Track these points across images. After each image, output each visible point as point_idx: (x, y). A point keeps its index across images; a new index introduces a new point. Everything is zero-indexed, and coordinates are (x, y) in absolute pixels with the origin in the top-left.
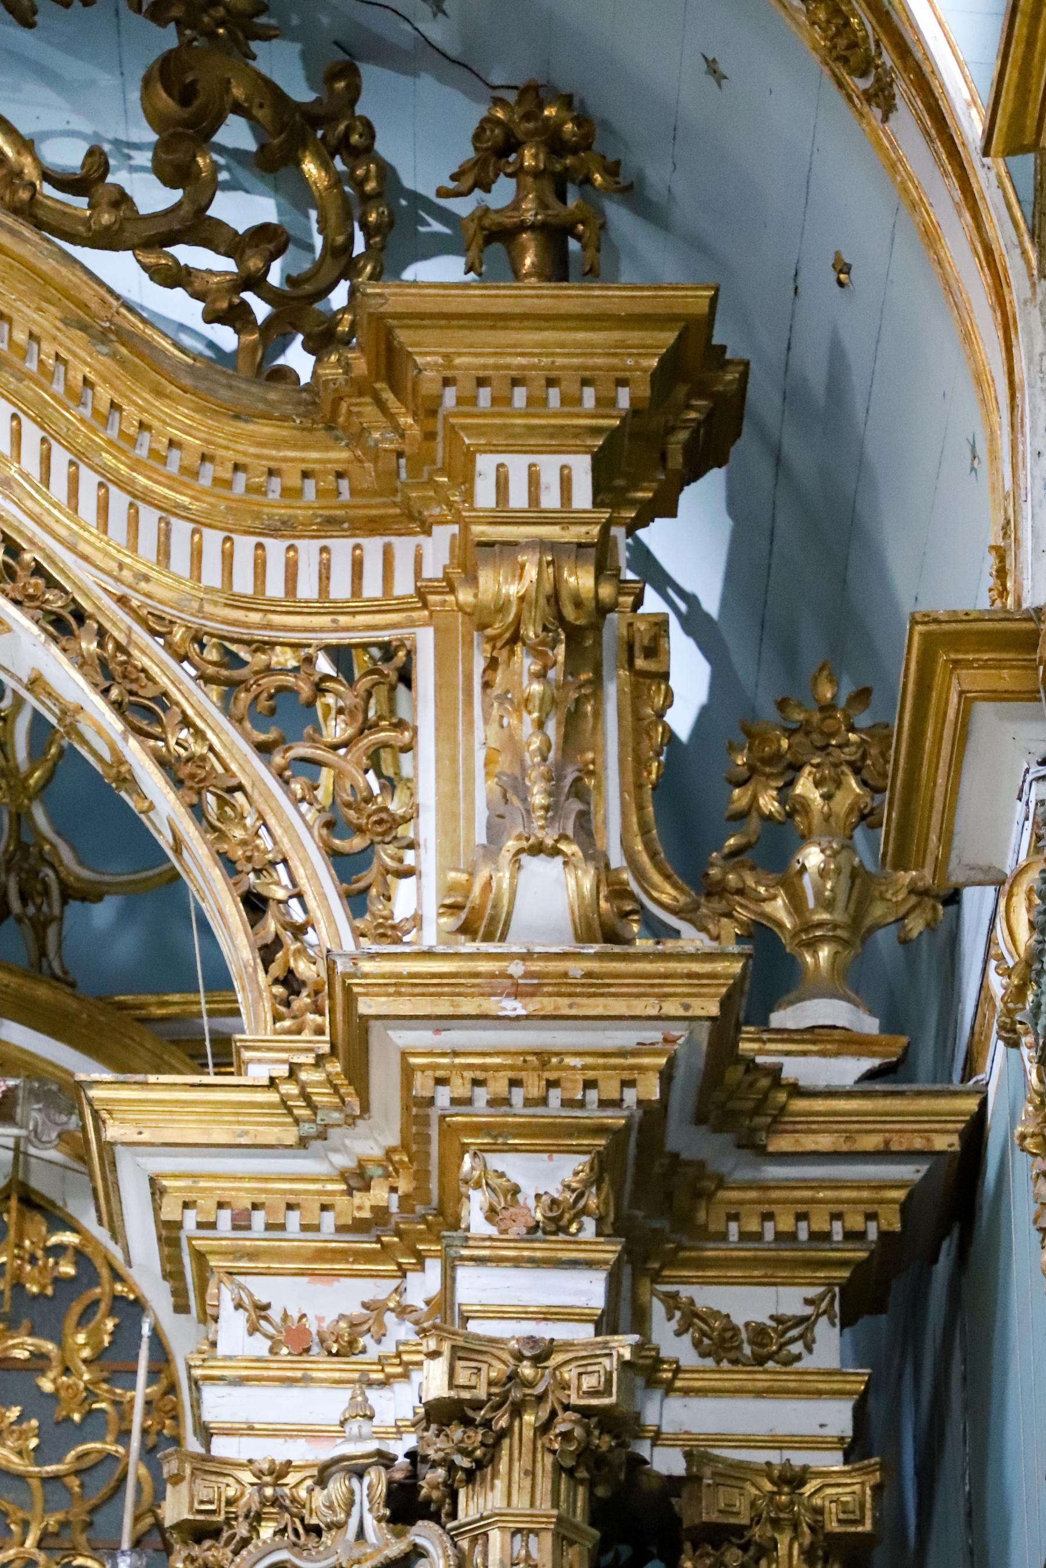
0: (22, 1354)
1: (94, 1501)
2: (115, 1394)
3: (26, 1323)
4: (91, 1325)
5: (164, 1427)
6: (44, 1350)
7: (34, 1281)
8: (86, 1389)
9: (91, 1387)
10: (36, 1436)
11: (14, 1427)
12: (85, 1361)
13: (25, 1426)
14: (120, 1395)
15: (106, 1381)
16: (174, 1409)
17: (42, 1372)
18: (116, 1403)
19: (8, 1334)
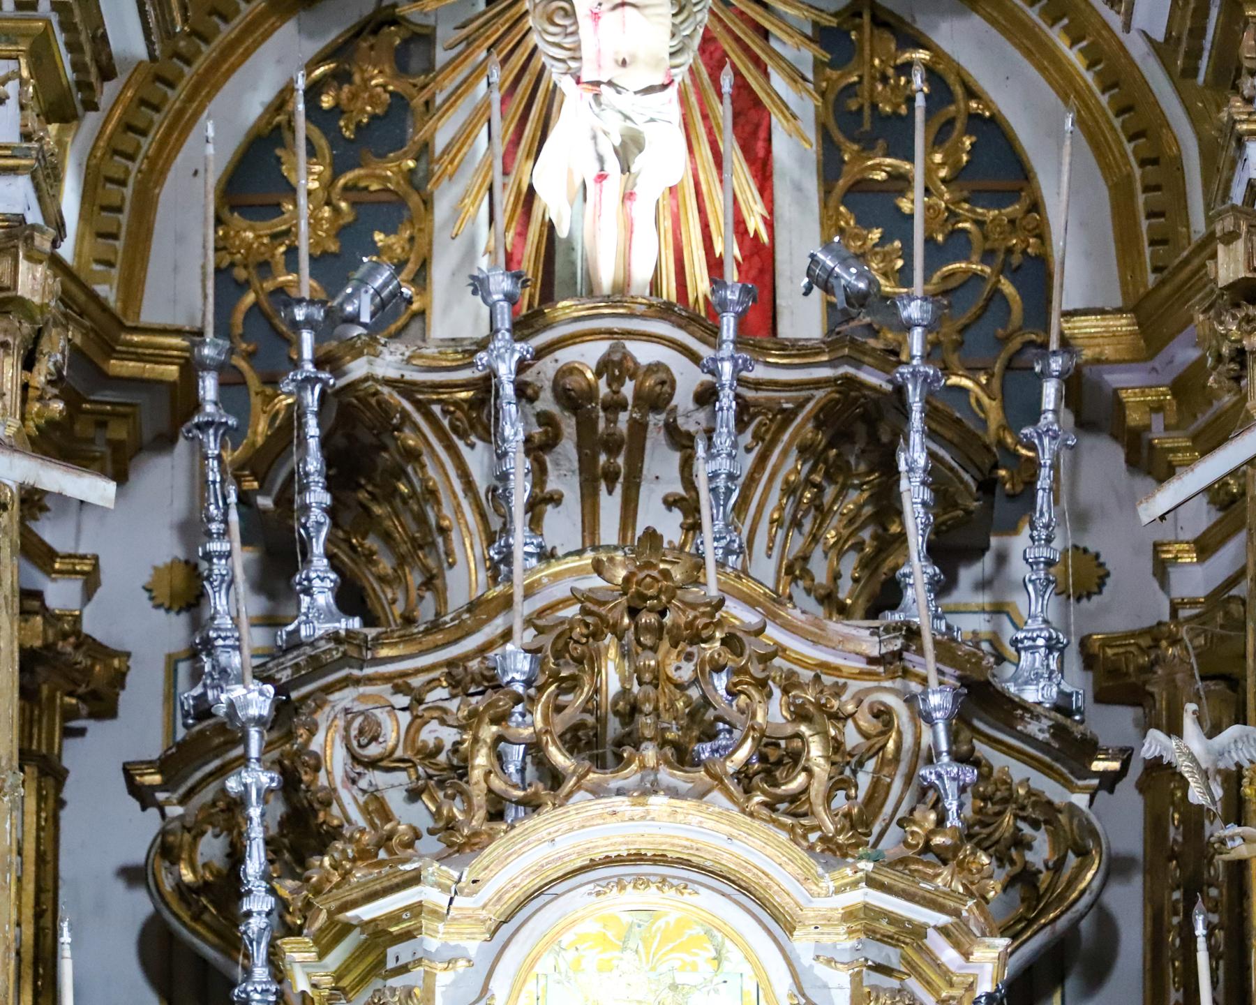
0: (880, 176)
1: (963, 321)
2: (975, 212)
3: (881, 143)
4: (947, 145)
5: (1028, 245)
6: (902, 171)
7: (888, 101)
8: (947, 208)
9: (952, 207)
10: (900, 257)
11: (877, 249)
12: (944, 181)
13: (888, 248)
14: (982, 214)
15: (966, 201)
16: (1037, 227)
17: (902, 193)
18: (979, 223)
19: (864, 155)
